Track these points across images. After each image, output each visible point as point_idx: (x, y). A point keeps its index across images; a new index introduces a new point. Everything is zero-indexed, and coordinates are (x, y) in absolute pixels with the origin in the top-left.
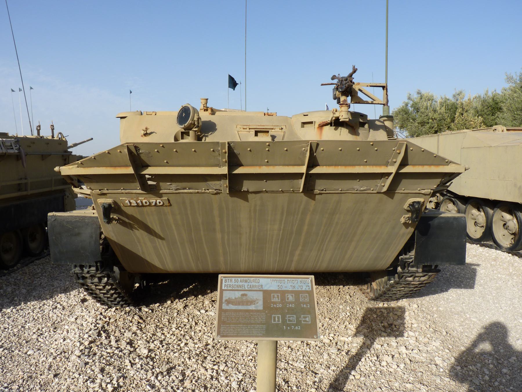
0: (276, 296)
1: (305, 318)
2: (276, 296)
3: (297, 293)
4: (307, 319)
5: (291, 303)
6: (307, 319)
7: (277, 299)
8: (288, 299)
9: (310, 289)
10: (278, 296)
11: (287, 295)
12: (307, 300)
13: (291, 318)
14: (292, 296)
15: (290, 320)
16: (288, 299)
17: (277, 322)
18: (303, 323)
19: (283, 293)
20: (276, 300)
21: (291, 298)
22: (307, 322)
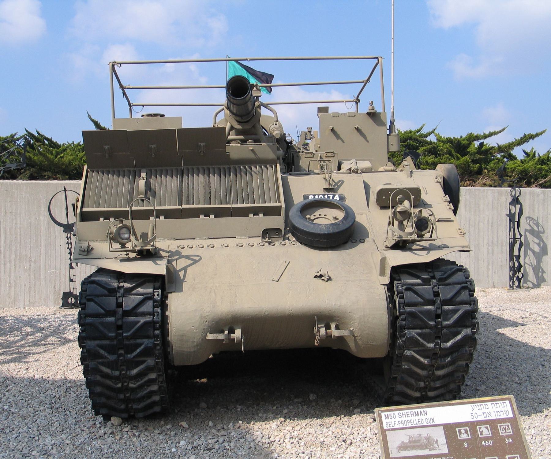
0: (463, 431)
2: (463, 431)
3: (492, 424)
5: (486, 439)
7: (466, 435)
8: (481, 434)
9: (511, 415)
10: (466, 430)
11: (480, 428)
12: (510, 432)
14: (487, 428)
16: (481, 434)
19: (472, 426)
20: (464, 436)
21: (486, 432)
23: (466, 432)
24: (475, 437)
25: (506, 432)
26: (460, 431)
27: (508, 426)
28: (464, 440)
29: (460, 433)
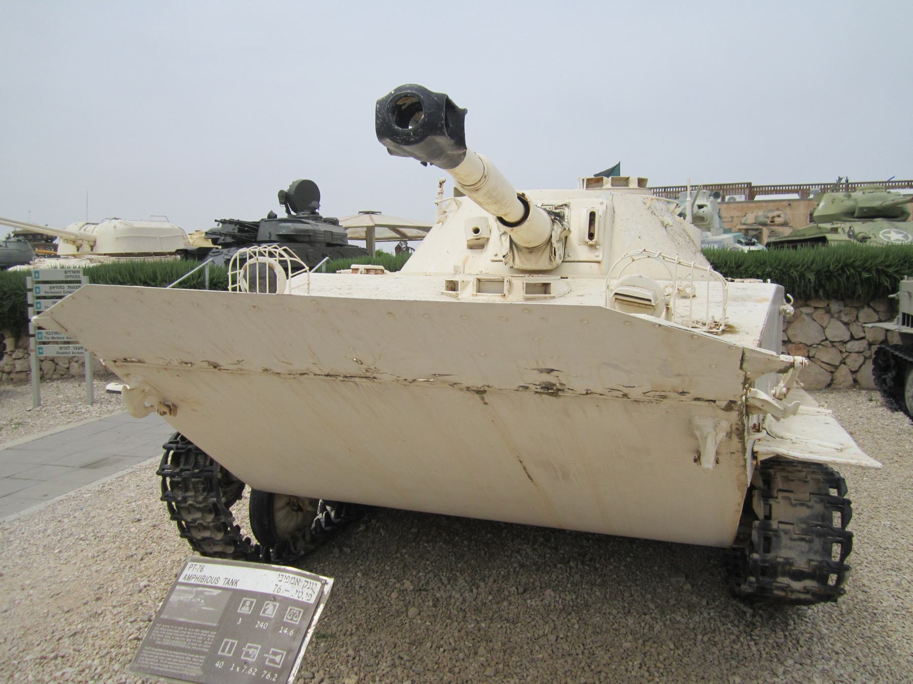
0: (248, 603)
1: (275, 654)
2: (248, 603)
4: (278, 658)
5: (266, 619)
6: (278, 658)
7: (247, 608)
8: (264, 612)
10: (252, 603)
13: (251, 651)
14: (275, 606)
15: (247, 655)
17: (226, 654)
18: (267, 663)
19: (262, 598)
20: (245, 610)
21: (270, 610)
22: (276, 663)
23: (250, 606)
24: (255, 616)
25: (292, 619)
26: (245, 601)
27: (300, 612)
28: (242, 615)
29: (243, 605)
